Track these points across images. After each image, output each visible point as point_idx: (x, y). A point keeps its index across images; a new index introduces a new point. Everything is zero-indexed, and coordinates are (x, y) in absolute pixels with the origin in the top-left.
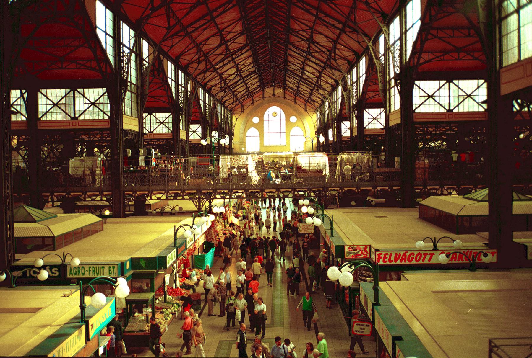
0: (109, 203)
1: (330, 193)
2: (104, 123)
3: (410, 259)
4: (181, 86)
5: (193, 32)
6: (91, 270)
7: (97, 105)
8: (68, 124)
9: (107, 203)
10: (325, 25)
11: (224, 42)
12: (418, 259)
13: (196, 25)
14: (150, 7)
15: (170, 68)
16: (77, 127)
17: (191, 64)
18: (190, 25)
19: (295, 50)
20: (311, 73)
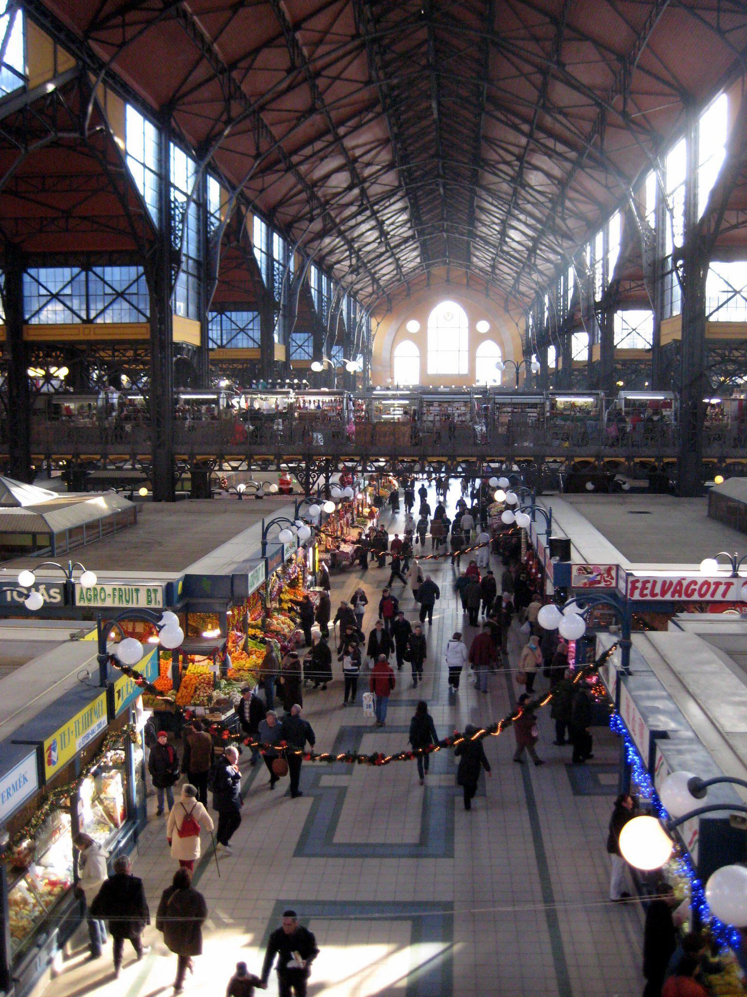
0: (147, 474)
1: (548, 467)
2: (138, 330)
3: (689, 591)
4: (278, 262)
5: (300, 163)
6: (117, 593)
7: (127, 297)
8: (75, 332)
9: (144, 475)
10: (546, 154)
11: (357, 181)
12: (703, 591)
13: (308, 151)
14: (224, 117)
15: (258, 228)
16: (92, 337)
17: (296, 222)
18: (296, 151)
19: (490, 200)
20: (518, 242)
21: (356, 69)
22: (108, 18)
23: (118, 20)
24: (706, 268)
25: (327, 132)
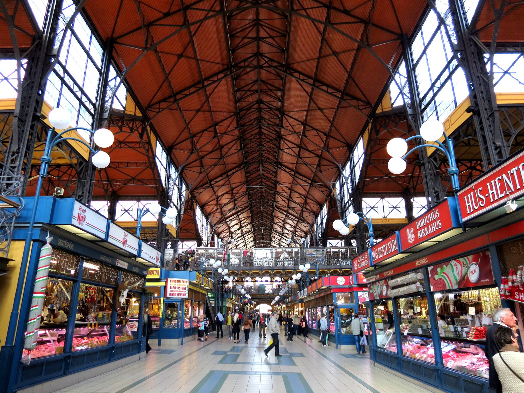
11: (233, 200)
13: (217, 180)
15: (198, 212)
18: (213, 180)
21: (236, 147)
22: (154, 104)
23: (157, 106)
24: (362, 200)
25: (225, 173)
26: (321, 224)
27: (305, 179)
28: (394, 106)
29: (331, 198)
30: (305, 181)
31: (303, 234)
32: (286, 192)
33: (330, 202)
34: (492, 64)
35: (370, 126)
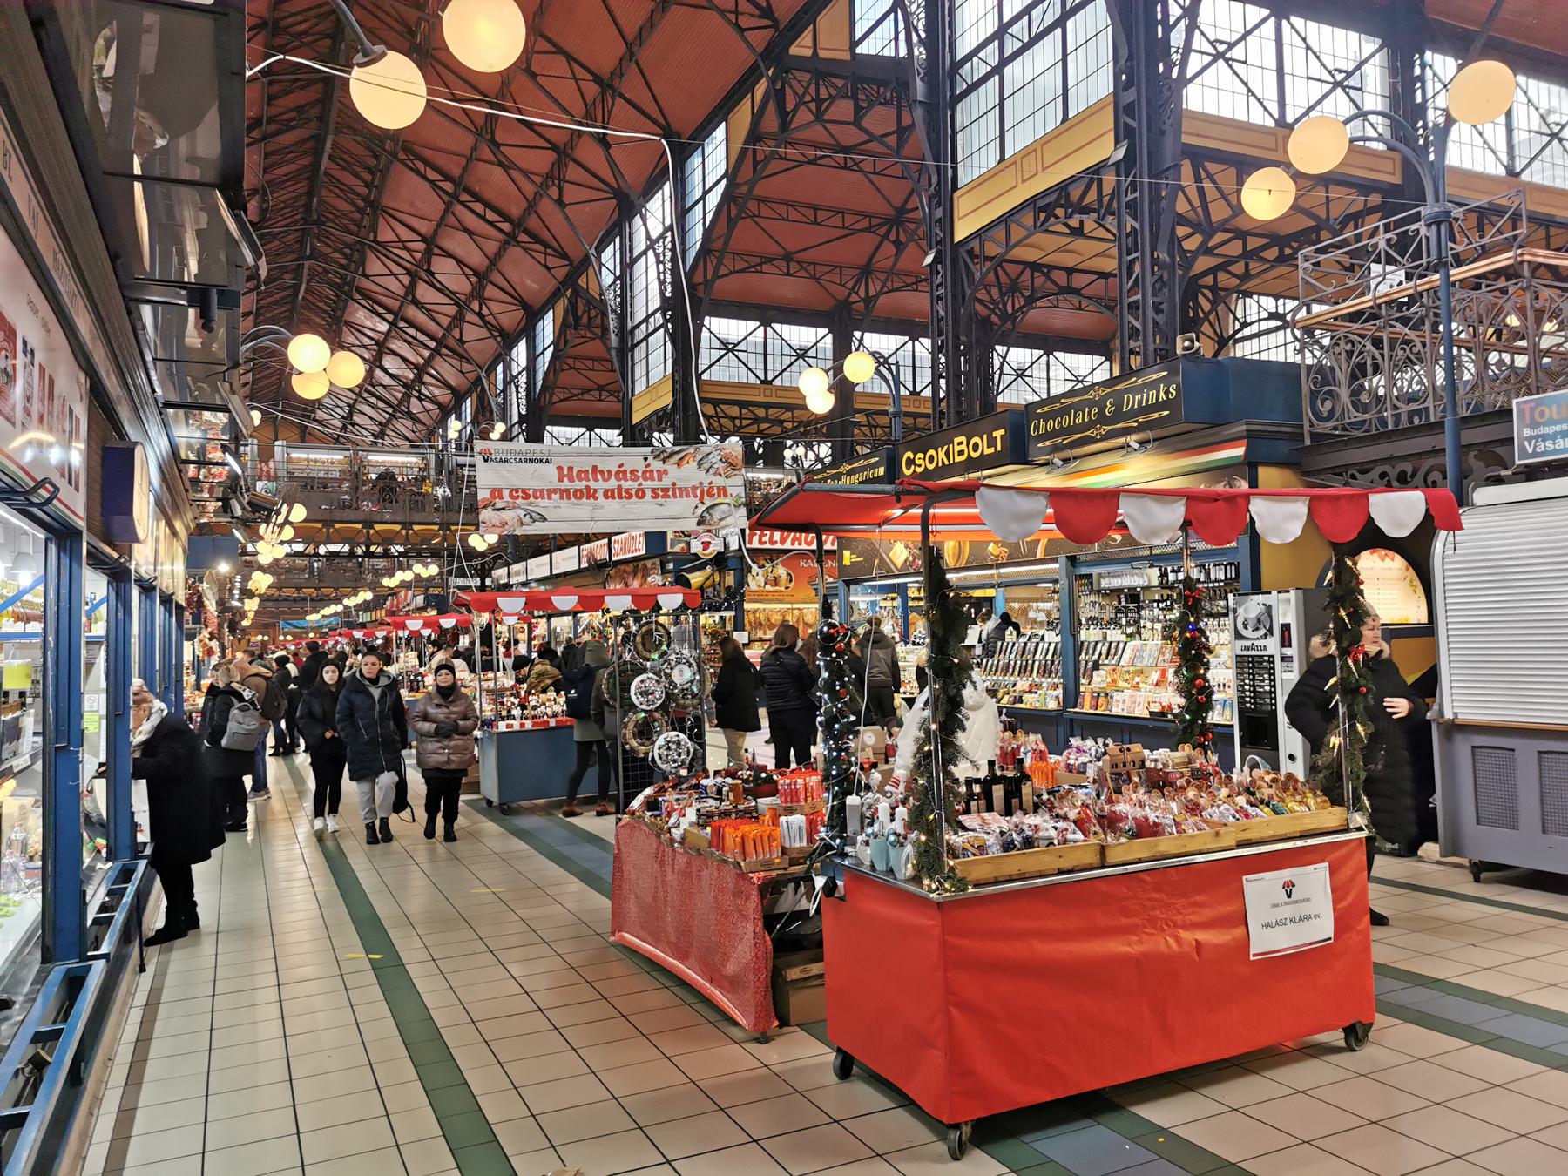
26: (531, 368)
27: (491, 216)
28: (858, 50)
29: (576, 293)
30: (492, 224)
31: (444, 396)
32: (406, 248)
33: (572, 308)
34: (1192, 28)
35: (761, 89)
